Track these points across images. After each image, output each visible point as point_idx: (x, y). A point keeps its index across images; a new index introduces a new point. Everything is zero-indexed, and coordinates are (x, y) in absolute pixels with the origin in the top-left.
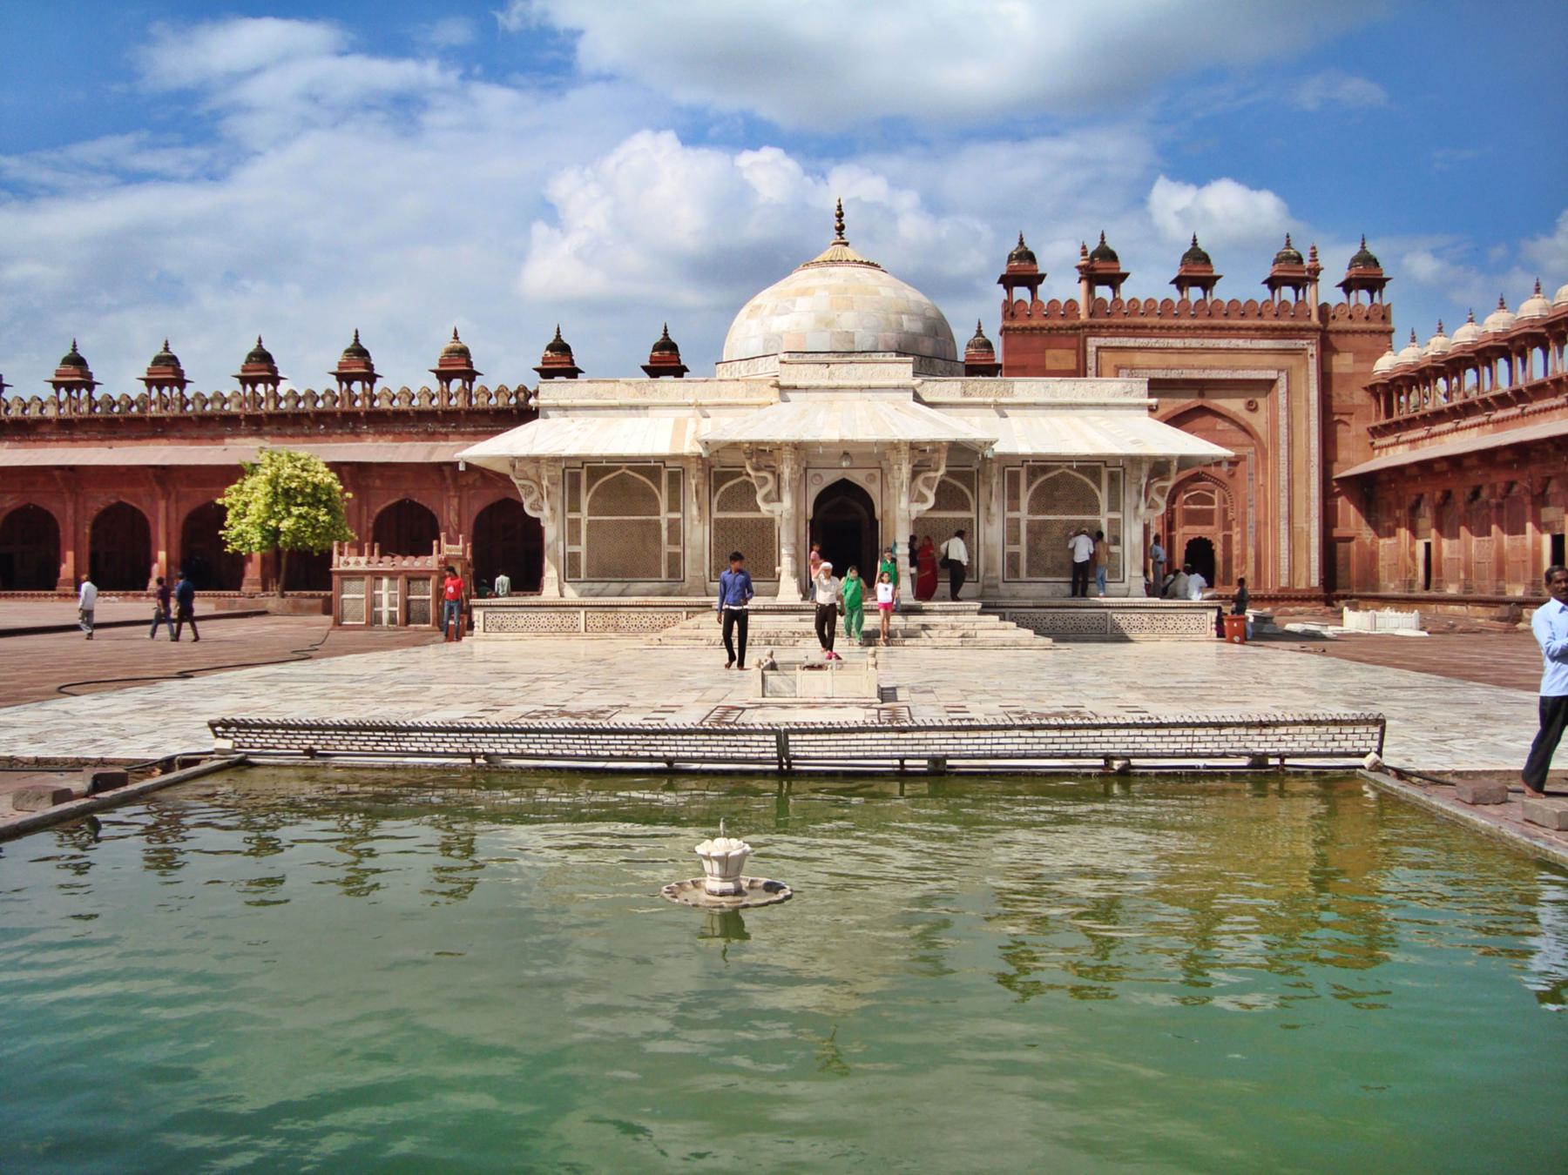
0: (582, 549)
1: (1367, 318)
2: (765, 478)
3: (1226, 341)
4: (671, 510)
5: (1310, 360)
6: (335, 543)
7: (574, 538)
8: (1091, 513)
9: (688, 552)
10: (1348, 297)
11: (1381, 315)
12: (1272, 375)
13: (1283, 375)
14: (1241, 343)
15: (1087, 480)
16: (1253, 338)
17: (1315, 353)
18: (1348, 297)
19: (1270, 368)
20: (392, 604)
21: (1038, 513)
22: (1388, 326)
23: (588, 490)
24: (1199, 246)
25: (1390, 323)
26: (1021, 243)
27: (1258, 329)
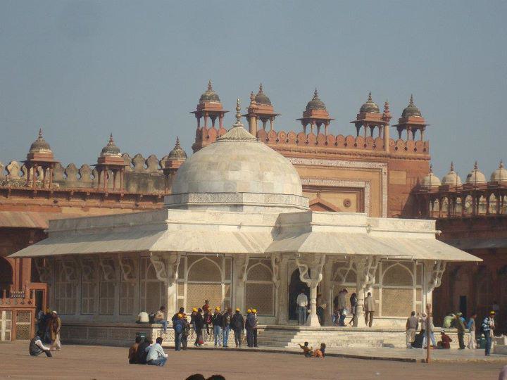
0: (184, 297)
1: (415, 150)
2: (304, 267)
3: (336, 161)
4: (226, 279)
5: (383, 176)
6: (5, 291)
7: (181, 292)
8: (408, 285)
9: (234, 300)
10: (400, 134)
11: (423, 148)
12: (361, 185)
13: (368, 185)
14: (344, 163)
15: (408, 269)
16: (351, 160)
17: (386, 171)
18: (400, 134)
19: (360, 180)
20: (8, 328)
21: (387, 285)
22: (427, 155)
23: (188, 267)
24: (319, 97)
25: (428, 153)
26: (210, 88)
27: (355, 154)
